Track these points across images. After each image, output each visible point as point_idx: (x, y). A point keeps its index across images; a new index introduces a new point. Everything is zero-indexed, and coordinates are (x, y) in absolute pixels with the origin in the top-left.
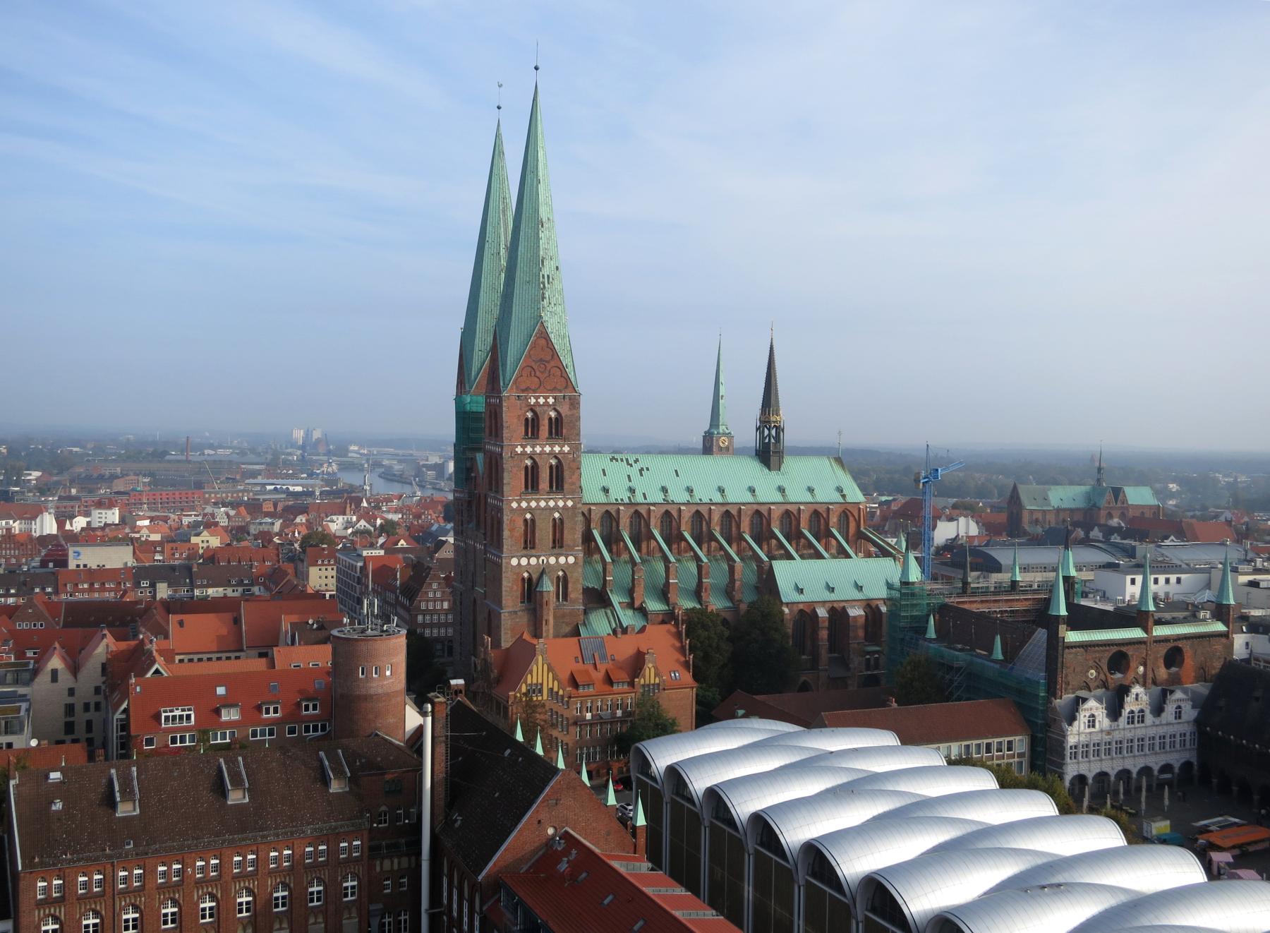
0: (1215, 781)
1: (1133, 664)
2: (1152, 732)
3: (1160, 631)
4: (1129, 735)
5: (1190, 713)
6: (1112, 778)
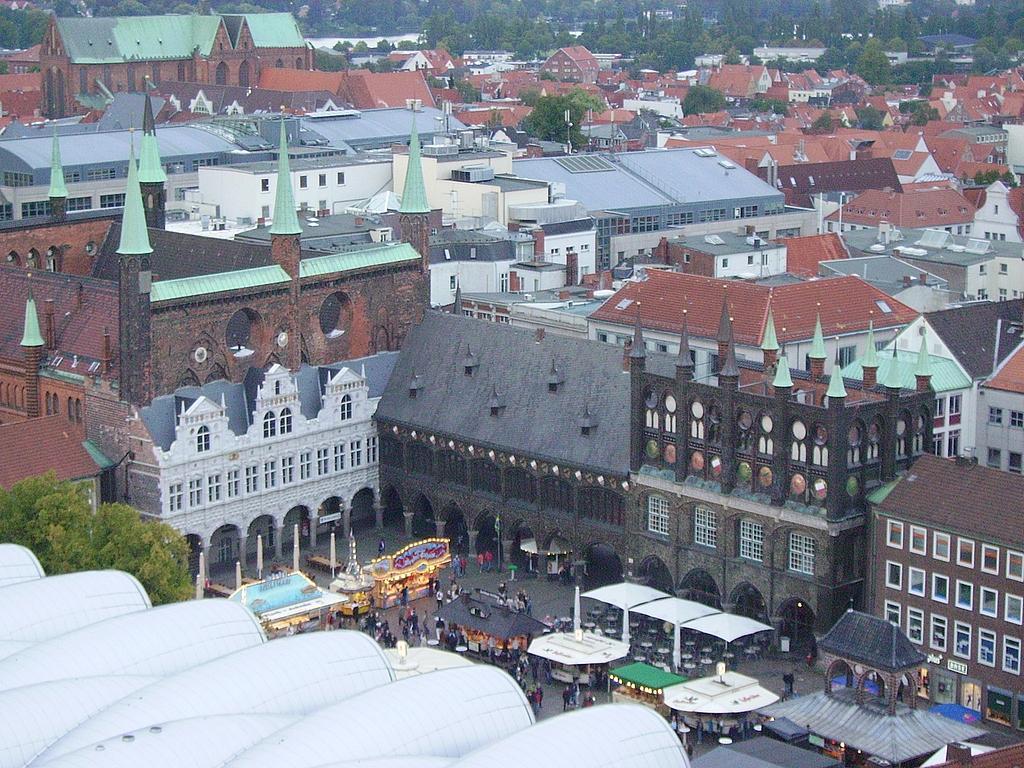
0: (408, 515)
1: (269, 331)
2: (304, 448)
3: (312, 268)
4: (268, 456)
5: (366, 407)
6: (244, 534)
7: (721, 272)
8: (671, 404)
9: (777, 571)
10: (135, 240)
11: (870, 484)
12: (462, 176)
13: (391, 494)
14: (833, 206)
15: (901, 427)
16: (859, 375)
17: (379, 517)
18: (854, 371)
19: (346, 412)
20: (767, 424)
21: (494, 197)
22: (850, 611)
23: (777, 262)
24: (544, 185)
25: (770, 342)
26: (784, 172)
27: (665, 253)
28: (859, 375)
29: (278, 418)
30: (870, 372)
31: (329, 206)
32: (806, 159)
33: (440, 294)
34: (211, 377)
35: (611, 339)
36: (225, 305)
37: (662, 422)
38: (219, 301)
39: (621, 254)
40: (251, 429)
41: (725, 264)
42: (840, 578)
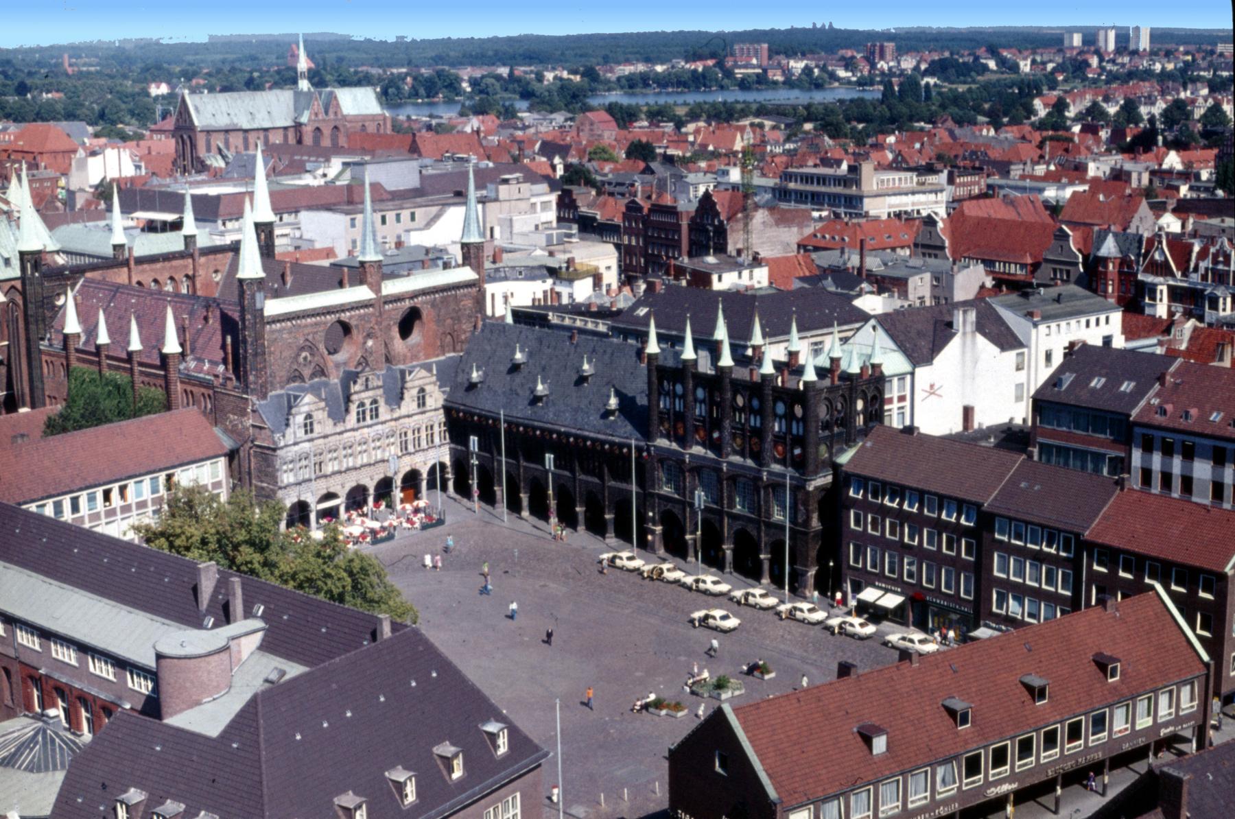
3: (391, 288)
5: (436, 398)
7: (717, 286)
18: (823, 361)
19: (422, 401)
28: (827, 364)
29: (368, 406)
34: (313, 375)
38: (318, 314)
40: (348, 418)
41: (720, 279)
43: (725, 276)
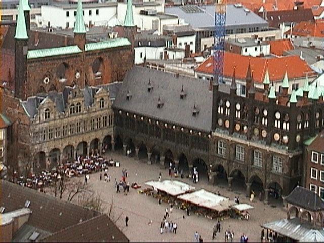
3: (90, 47)
7: (244, 53)
8: (228, 104)
9: (267, 170)
10: (21, 33)
11: (304, 138)
12: (144, 13)
13: (118, 139)
14: (288, 29)
15: (318, 116)
16: (301, 94)
17: (113, 146)
18: (300, 93)
20: (266, 113)
21: (157, 22)
22: (298, 187)
23: (266, 50)
24: (177, 17)
25: (267, 80)
26: (270, 14)
27: (223, 45)
28: (301, 94)
30: (306, 93)
31: (92, 23)
32: (277, 9)
33: (138, 60)
34: (50, 90)
35: (204, 78)
36: (56, 61)
37: (224, 111)
39: (205, 46)
41: (246, 50)
42: (293, 174)
43: (248, 49)
